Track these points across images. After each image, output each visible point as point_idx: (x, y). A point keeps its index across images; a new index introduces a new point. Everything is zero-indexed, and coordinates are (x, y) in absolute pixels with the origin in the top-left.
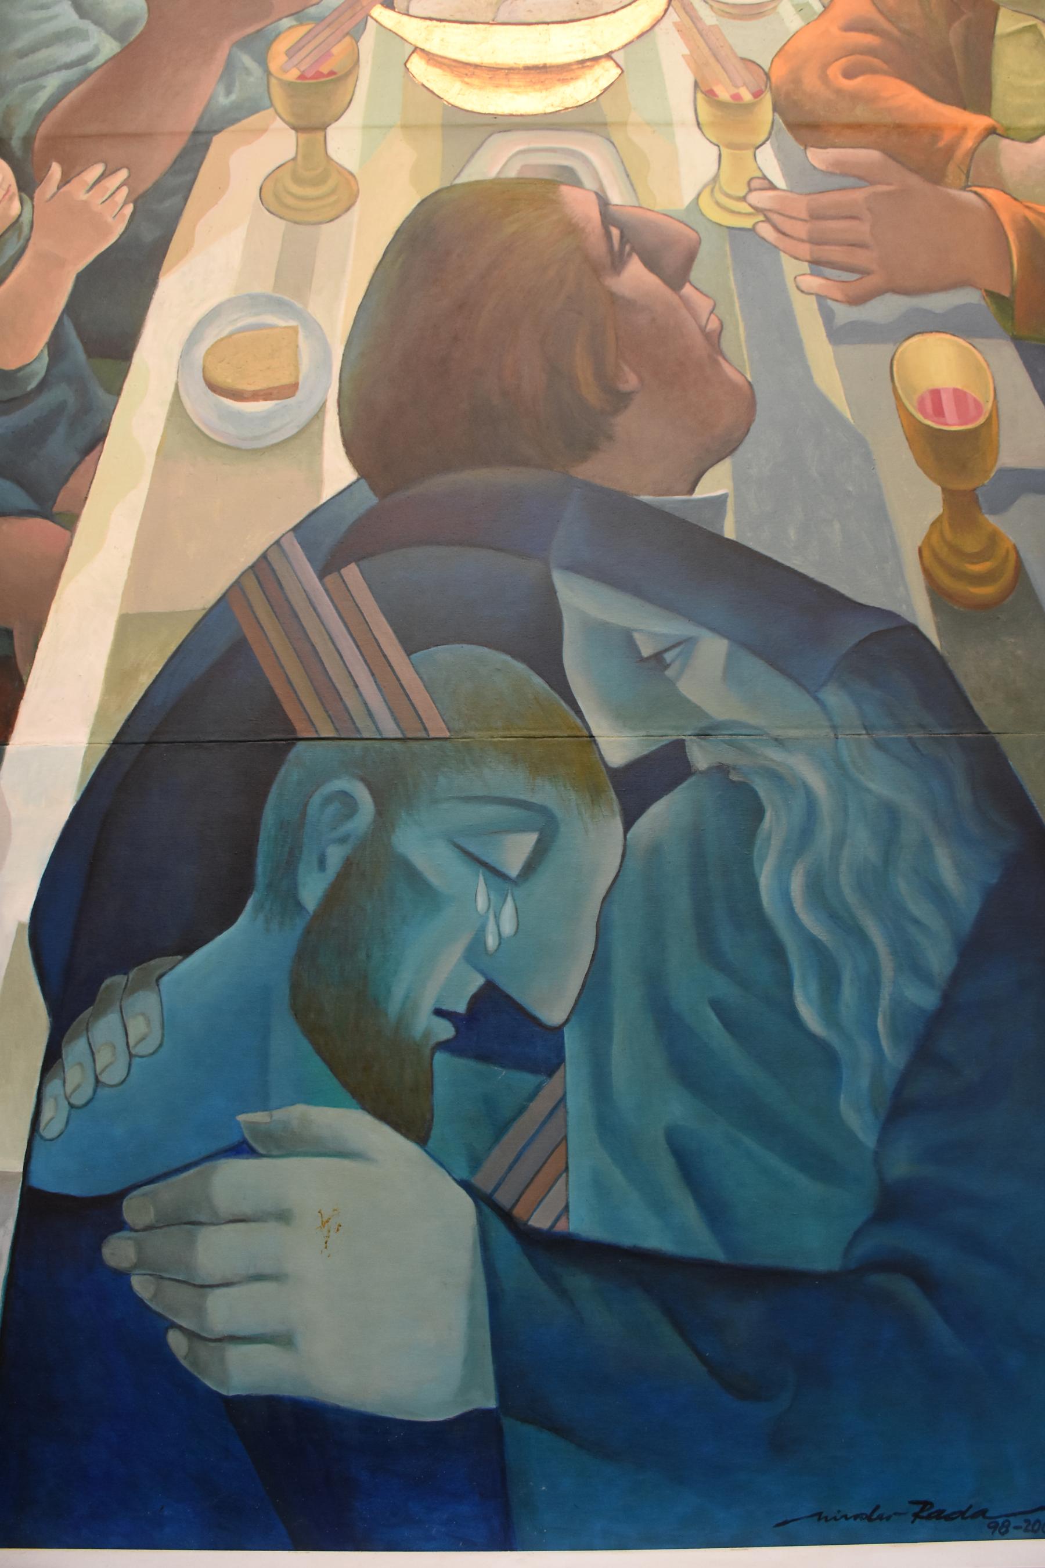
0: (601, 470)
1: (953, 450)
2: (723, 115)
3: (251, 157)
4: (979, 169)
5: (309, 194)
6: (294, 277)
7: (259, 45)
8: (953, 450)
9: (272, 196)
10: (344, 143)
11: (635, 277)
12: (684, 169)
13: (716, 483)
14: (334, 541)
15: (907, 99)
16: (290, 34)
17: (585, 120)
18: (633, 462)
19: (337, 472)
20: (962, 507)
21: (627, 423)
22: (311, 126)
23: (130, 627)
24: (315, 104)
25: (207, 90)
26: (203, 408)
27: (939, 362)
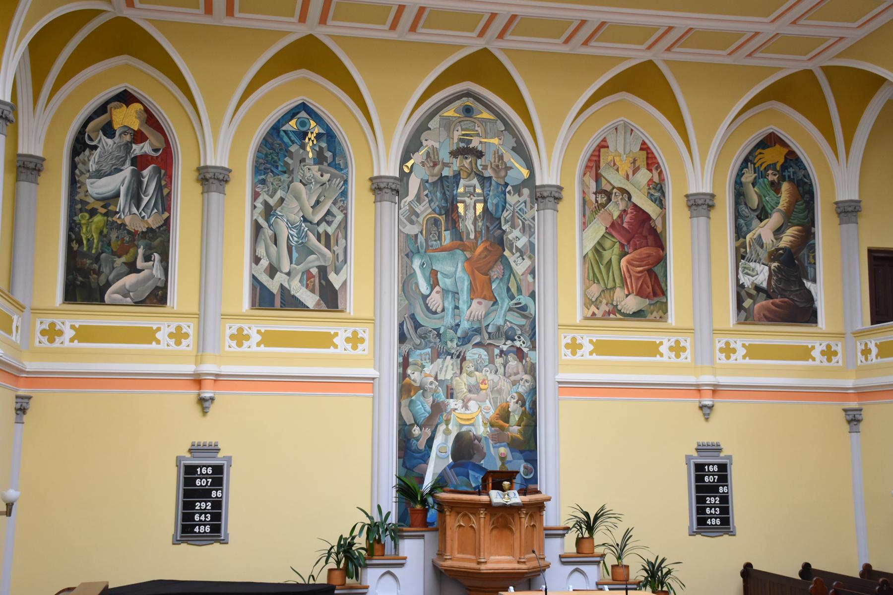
0: (473, 461)
1: (503, 459)
2: (485, 424)
3: (442, 428)
4: (508, 430)
5: (447, 432)
6: (446, 441)
7: (442, 415)
8: (503, 459)
9: (444, 432)
10: (450, 427)
11: (476, 441)
12: (481, 430)
13: (482, 462)
14: (451, 467)
15: (501, 422)
16: (445, 414)
17: (472, 425)
18: (475, 460)
19: (451, 460)
20: (503, 464)
21: (476, 457)
22: (447, 425)
23: (434, 474)
24: (447, 422)
25: (437, 421)
26: (439, 454)
27: (502, 450)
